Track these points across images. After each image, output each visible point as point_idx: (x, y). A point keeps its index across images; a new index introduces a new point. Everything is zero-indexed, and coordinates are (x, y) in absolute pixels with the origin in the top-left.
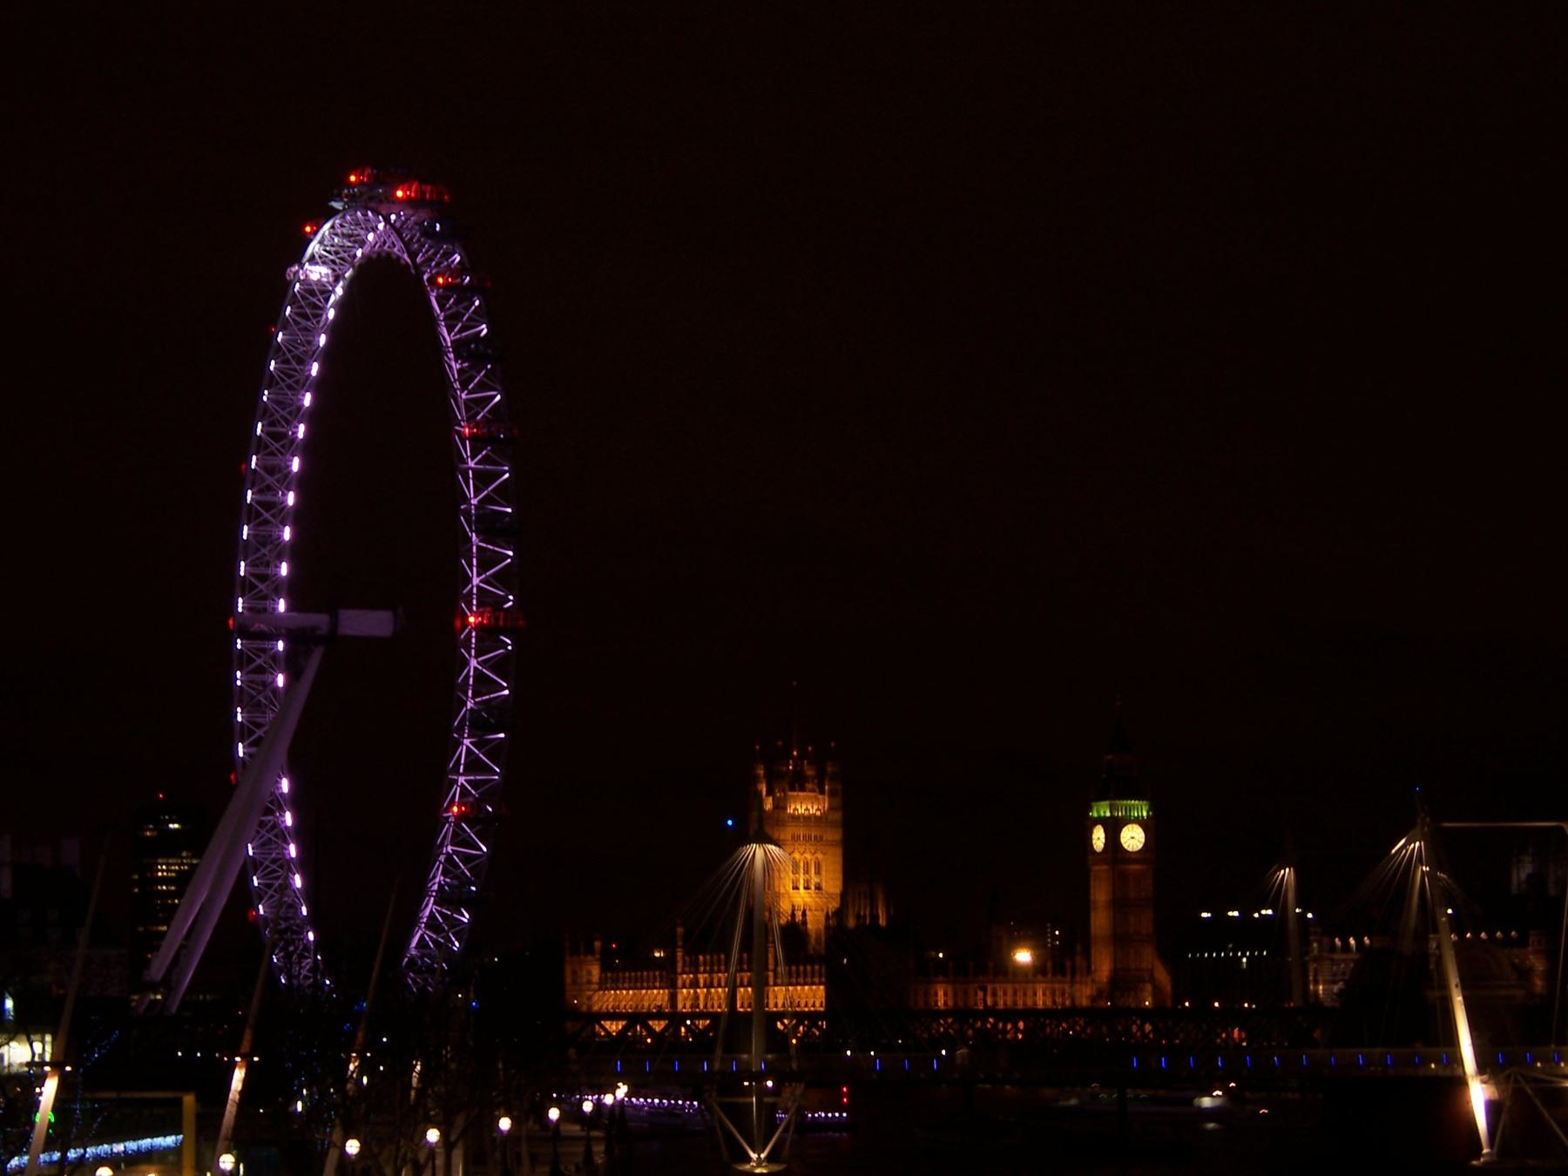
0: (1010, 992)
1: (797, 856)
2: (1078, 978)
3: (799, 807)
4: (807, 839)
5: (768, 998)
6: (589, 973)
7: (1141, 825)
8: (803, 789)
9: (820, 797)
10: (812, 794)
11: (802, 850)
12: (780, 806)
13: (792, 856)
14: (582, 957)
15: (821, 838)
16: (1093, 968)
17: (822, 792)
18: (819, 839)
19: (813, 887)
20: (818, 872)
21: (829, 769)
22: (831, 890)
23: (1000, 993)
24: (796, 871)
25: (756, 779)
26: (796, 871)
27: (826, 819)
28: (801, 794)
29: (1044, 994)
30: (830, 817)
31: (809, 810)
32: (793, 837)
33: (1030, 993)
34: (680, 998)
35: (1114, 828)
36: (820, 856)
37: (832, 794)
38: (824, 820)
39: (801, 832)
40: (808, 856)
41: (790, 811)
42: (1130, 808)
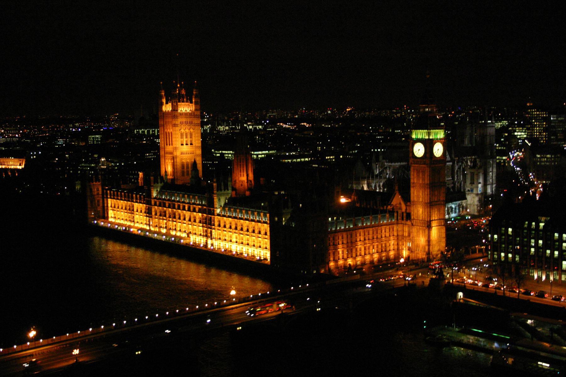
0: (371, 232)
1: (182, 130)
2: (400, 221)
3: (182, 109)
4: (186, 123)
5: (214, 221)
6: (98, 190)
7: (441, 143)
8: (183, 102)
9: (191, 104)
10: (187, 103)
11: (184, 128)
12: (175, 109)
13: (180, 131)
14: (94, 183)
15: (192, 123)
16: (412, 218)
17: (191, 102)
18: (191, 123)
19: (189, 144)
20: (191, 138)
21: (194, 93)
22: (197, 145)
23: (367, 234)
24: (182, 138)
25: (161, 97)
26: (182, 138)
27: (194, 114)
28: (183, 103)
29: (385, 232)
30: (196, 113)
31: (187, 111)
32: (181, 123)
33: (379, 231)
34: (153, 210)
35: (429, 144)
36: (192, 130)
37: (196, 103)
38: (193, 115)
39: (184, 120)
40: (187, 130)
41: (179, 111)
42: (436, 134)
